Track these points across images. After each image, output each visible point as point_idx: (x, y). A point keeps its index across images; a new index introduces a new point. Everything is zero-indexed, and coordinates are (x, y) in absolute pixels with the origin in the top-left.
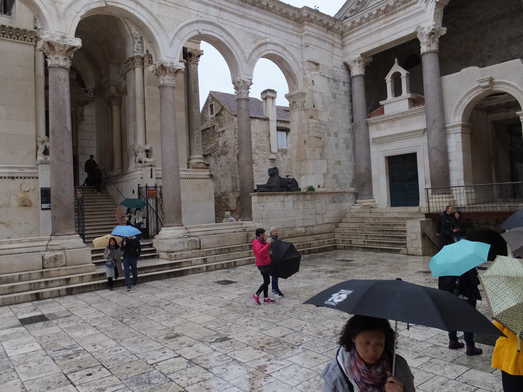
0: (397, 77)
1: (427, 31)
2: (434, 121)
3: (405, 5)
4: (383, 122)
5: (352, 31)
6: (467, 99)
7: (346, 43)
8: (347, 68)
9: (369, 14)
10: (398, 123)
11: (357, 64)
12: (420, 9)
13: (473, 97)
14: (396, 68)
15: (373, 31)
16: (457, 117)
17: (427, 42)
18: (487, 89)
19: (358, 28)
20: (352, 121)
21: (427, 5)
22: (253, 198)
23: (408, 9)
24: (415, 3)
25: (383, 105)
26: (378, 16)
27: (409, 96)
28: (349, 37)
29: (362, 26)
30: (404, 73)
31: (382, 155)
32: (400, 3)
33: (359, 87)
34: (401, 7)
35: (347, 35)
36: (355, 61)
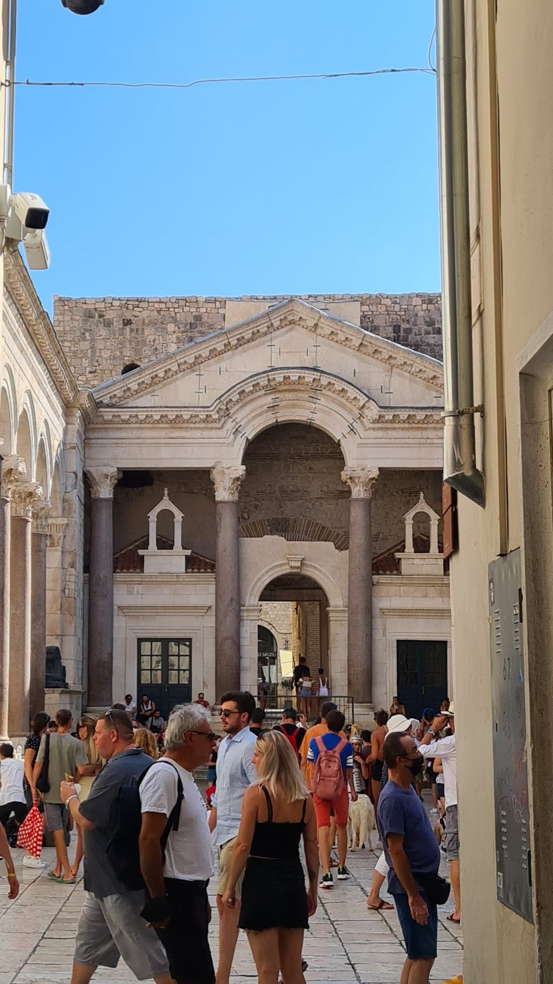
0: (166, 518)
1: (234, 476)
2: (232, 599)
3: (203, 425)
4: (140, 583)
5: (106, 426)
6: (267, 576)
7: (93, 441)
8: (88, 481)
9: (147, 416)
10: (166, 589)
11: (108, 481)
12: (226, 441)
13: (275, 576)
14: (166, 504)
15: (148, 441)
16: (253, 597)
17: (229, 488)
18: (295, 570)
19: (120, 426)
20: (87, 568)
21: (235, 438)
22: (47, 696)
23: (206, 433)
24: (219, 429)
25: (143, 556)
26: (158, 423)
27: (188, 552)
28: (100, 435)
29: (127, 426)
30: (178, 515)
31: (134, 636)
32: (197, 419)
33: (105, 518)
34: (197, 425)
35: (94, 429)
36: (106, 476)
